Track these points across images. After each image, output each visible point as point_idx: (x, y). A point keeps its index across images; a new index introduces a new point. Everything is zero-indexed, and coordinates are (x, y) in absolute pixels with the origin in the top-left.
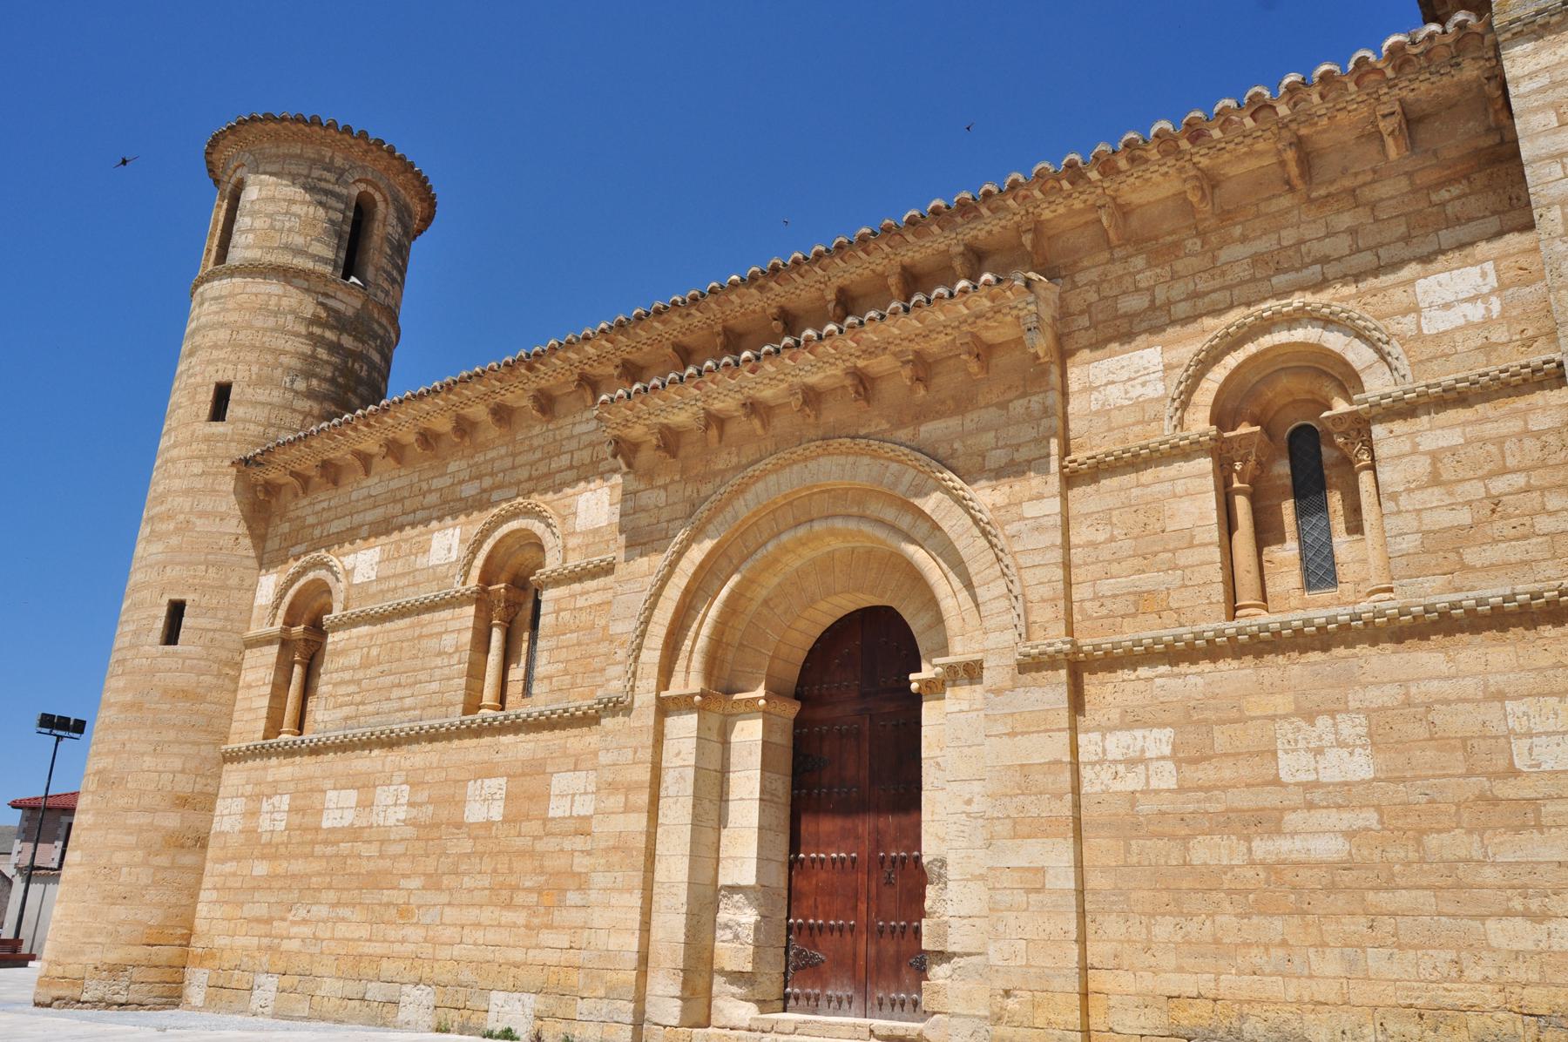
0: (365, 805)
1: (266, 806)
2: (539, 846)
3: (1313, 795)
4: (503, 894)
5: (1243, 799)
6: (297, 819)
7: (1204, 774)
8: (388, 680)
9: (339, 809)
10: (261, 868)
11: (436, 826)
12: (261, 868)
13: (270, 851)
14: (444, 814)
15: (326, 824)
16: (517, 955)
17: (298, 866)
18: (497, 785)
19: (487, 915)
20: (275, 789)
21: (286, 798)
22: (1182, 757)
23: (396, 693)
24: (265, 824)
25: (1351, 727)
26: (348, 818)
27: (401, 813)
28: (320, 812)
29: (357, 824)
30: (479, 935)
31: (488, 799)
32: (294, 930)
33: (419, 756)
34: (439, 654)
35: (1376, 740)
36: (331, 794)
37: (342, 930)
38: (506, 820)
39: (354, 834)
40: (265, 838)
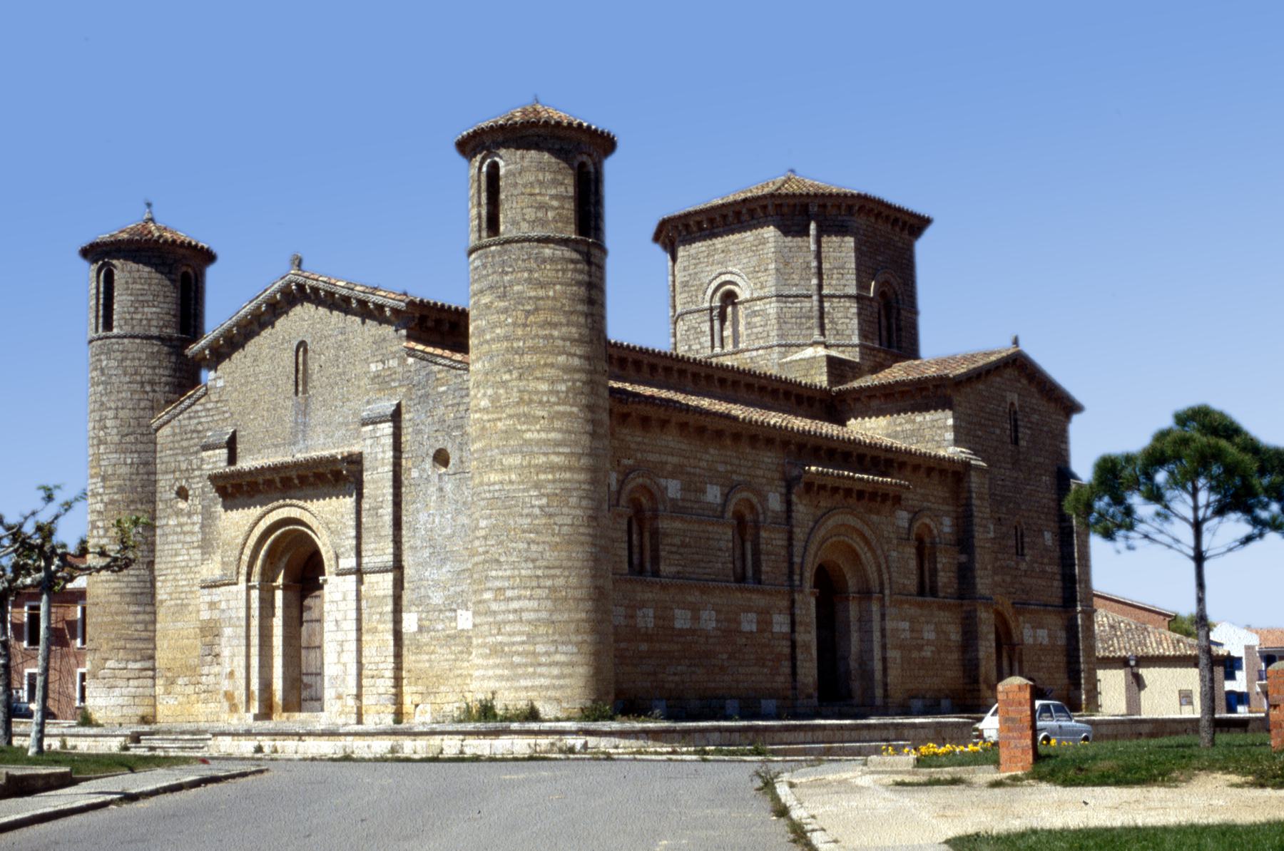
0: (696, 618)
1: (639, 613)
3: (929, 642)
5: (919, 642)
6: (661, 623)
7: (915, 635)
8: (696, 557)
9: (682, 620)
10: (644, 647)
11: (730, 632)
12: (644, 647)
13: (648, 637)
14: (733, 626)
15: (678, 625)
16: (769, 686)
17: (665, 647)
18: (752, 616)
19: (756, 669)
20: (643, 605)
21: (651, 612)
22: (912, 631)
23: (703, 565)
24: (640, 623)
25: (933, 627)
26: (688, 626)
27: (714, 625)
28: (673, 619)
29: (696, 626)
32: (671, 678)
34: (720, 550)
35: (937, 633)
36: (678, 612)
39: (692, 631)
40: (643, 630)
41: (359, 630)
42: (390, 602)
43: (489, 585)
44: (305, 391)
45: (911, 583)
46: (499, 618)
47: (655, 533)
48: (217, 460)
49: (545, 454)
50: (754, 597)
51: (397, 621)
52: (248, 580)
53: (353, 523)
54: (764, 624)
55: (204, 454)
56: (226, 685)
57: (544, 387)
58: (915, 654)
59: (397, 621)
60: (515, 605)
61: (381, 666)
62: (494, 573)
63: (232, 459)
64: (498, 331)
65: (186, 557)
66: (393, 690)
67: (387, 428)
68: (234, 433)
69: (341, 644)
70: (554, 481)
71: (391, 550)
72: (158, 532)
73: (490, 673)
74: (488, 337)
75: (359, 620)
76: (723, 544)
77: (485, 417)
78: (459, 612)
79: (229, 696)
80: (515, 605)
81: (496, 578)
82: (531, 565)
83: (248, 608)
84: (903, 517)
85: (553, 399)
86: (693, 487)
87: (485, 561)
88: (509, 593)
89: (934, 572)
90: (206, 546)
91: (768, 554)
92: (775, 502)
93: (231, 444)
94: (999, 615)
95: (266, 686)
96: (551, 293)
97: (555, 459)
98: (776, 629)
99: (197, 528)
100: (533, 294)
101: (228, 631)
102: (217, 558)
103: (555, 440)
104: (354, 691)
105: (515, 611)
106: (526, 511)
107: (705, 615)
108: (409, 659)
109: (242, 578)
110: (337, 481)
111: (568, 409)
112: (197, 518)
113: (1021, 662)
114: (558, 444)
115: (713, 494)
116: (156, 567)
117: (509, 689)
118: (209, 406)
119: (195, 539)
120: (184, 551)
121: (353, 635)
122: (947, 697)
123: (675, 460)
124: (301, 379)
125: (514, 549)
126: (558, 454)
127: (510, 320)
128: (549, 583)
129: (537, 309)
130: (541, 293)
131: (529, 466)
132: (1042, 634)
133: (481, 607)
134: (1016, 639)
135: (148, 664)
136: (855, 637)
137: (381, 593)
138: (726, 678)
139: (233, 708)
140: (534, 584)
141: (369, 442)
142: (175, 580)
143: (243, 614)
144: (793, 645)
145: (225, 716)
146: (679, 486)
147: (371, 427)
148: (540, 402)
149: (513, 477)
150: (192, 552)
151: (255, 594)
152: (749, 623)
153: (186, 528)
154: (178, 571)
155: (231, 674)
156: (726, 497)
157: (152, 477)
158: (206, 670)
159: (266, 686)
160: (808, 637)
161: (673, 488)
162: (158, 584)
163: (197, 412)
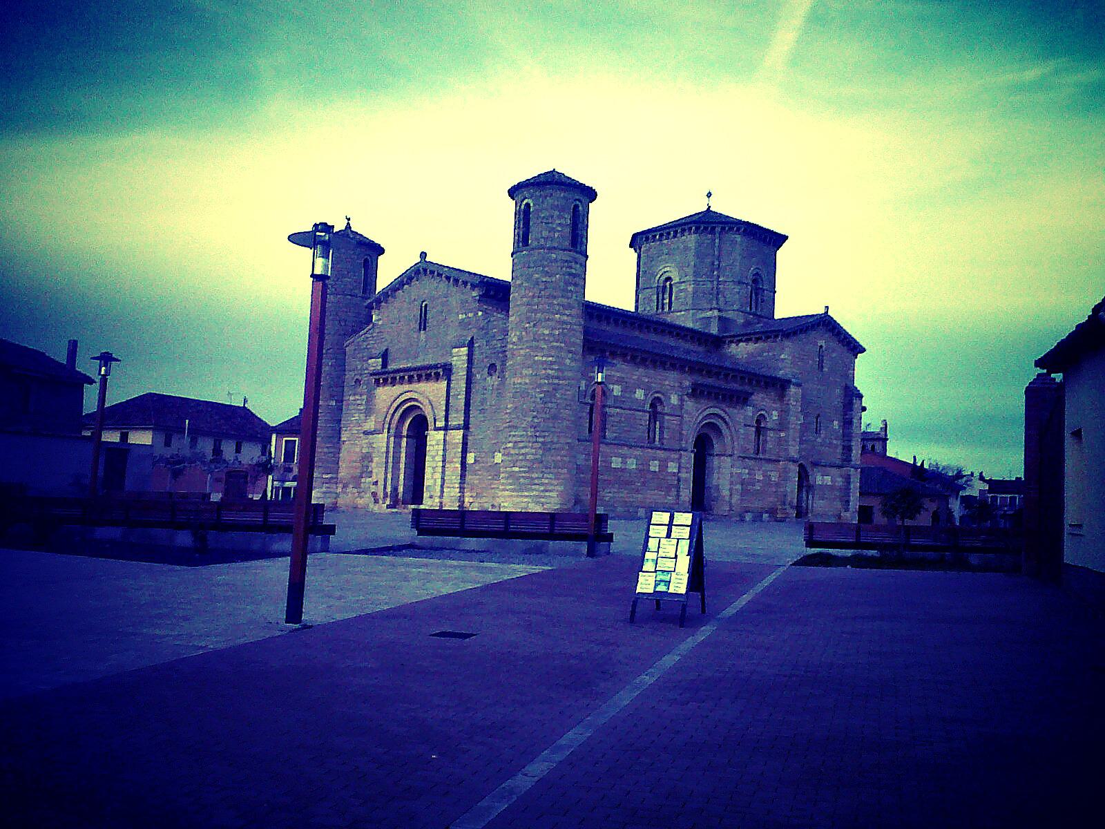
0: (624, 462)
2: (666, 478)
3: (759, 481)
4: (659, 488)
11: (643, 471)
18: (657, 462)
27: (634, 467)
30: (655, 497)
31: (655, 466)
32: (607, 495)
33: (638, 452)
37: (621, 495)
38: (659, 471)
39: (622, 470)
41: (444, 461)
42: (461, 446)
43: (510, 439)
44: (425, 329)
45: (751, 447)
46: (515, 458)
47: (604, 415)
48: (376, 364)
49: (545, 369)
50: (658, 451)
51: (464, 458)
52: (388, 432)
53: (444, 402)
54: (663, 467)
55: (370, 361)
56: (373, 489)
57: (547, 332)
58: (749, 487)
59: (464, 458)
60: (523, 451)
61: (453, 482)
62: (513, 433)
63: (385, 365)
64: (524, 299)
65: (357, 418)
66: (459, 494)
67: (465, 350)
68: (387, 350)
69: (434, 468)
70: (549, 384)
71: (463, 418)
72: (344, 403)
73: (508, 487)
74: (518, 303)
75: (444, 456)
76: (643, 423)
77: (515, 347)
78: (496, 453)
79: (374, 494)
80: (523, 451)
81: (514, 436)
82: (533, 430)
83: (388, 447)
84: (749, 410)
85: (552, 339)
86: (628, 389)
87: (509, 427)
88: (521, 445)
89: (765, 441)
90: (369, 411)
91: (668, 428)
92: (674, 400)
93: (385, 356)
94: (801, 466)
95: (395, 489)
96: (554, 280)
97: (550, 372)
98: (670, 470)
99: (364, 403)
100: (544, 280)
101: (375, 460)
102: (373, 418)
103: (551, 362)
104: (439, 494)
105: (523, 454)
106: (533, 399)
107: (629, 461)
108: (468, 478)
109: (386, 431)
110: (437, 380)
111: (558, 344)
112: (365, 397)
113: (813, 494)
114: (552, 363)
115: (640, 394)
116: (342, 422)
117: (517, 496)
118: (375, 334)
119: (362, 408)
120: (357, 415)
121: (440, 464)
122: (767, 512)
123: (618, 375)
124: (423, 324)
125: (525, 420)
126: (552, 369)
127: (530, 294)
128: (541, 440)
129: (546, 288)
130: (549, 280)
131: (536, 375)
132: (828, 478)
133: (507, 451)
134: (811, 482)
135: (334, 476)
136: (716, 476)
137: (458, 441)
138: (640, 496)
139: (376, 501)
140: (534, 440)
141: (455, 358)
142: (350, 430)
143: (384, 449)
144: (679, 480)
145: (371, 506)
146: (620, 389)
147: (457, 350)
148: (544, 339)
149: (527, 381)
150: (361, 415)
151: (392, 439)
152: (654, 466)
153: (359, 402)
154: (352, 425)
155: (376, 483)
156: (646, 395)
157: (342, 373)
158: (363, 480)
159: (395, 489)
160: (688, 475)
161: (617, 390)
162: (343, 432)
163: (367, 338)
